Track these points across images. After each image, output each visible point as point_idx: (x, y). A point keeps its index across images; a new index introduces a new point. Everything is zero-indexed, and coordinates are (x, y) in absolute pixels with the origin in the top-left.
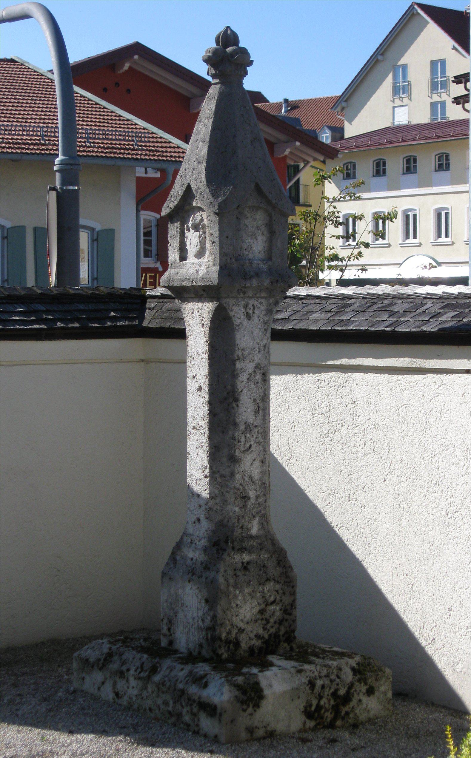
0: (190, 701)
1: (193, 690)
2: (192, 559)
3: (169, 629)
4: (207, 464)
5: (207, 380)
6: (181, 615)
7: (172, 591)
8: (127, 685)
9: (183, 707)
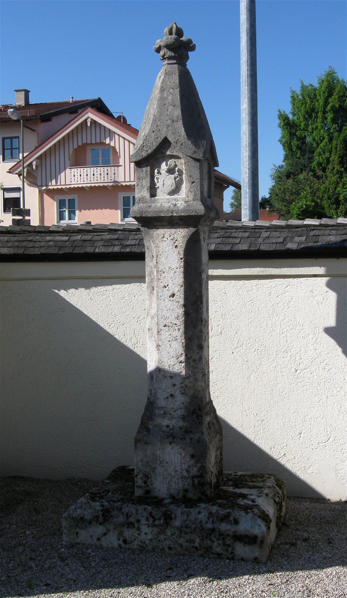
0: (223, 536)
1: (224, 527)
2: (168, 426)
3: (145, 482)
4: (183, 353)
5: (183, 288)
6: (160, 470)
7: (149, 452)
8: (138, 532)
9: (213, 542)
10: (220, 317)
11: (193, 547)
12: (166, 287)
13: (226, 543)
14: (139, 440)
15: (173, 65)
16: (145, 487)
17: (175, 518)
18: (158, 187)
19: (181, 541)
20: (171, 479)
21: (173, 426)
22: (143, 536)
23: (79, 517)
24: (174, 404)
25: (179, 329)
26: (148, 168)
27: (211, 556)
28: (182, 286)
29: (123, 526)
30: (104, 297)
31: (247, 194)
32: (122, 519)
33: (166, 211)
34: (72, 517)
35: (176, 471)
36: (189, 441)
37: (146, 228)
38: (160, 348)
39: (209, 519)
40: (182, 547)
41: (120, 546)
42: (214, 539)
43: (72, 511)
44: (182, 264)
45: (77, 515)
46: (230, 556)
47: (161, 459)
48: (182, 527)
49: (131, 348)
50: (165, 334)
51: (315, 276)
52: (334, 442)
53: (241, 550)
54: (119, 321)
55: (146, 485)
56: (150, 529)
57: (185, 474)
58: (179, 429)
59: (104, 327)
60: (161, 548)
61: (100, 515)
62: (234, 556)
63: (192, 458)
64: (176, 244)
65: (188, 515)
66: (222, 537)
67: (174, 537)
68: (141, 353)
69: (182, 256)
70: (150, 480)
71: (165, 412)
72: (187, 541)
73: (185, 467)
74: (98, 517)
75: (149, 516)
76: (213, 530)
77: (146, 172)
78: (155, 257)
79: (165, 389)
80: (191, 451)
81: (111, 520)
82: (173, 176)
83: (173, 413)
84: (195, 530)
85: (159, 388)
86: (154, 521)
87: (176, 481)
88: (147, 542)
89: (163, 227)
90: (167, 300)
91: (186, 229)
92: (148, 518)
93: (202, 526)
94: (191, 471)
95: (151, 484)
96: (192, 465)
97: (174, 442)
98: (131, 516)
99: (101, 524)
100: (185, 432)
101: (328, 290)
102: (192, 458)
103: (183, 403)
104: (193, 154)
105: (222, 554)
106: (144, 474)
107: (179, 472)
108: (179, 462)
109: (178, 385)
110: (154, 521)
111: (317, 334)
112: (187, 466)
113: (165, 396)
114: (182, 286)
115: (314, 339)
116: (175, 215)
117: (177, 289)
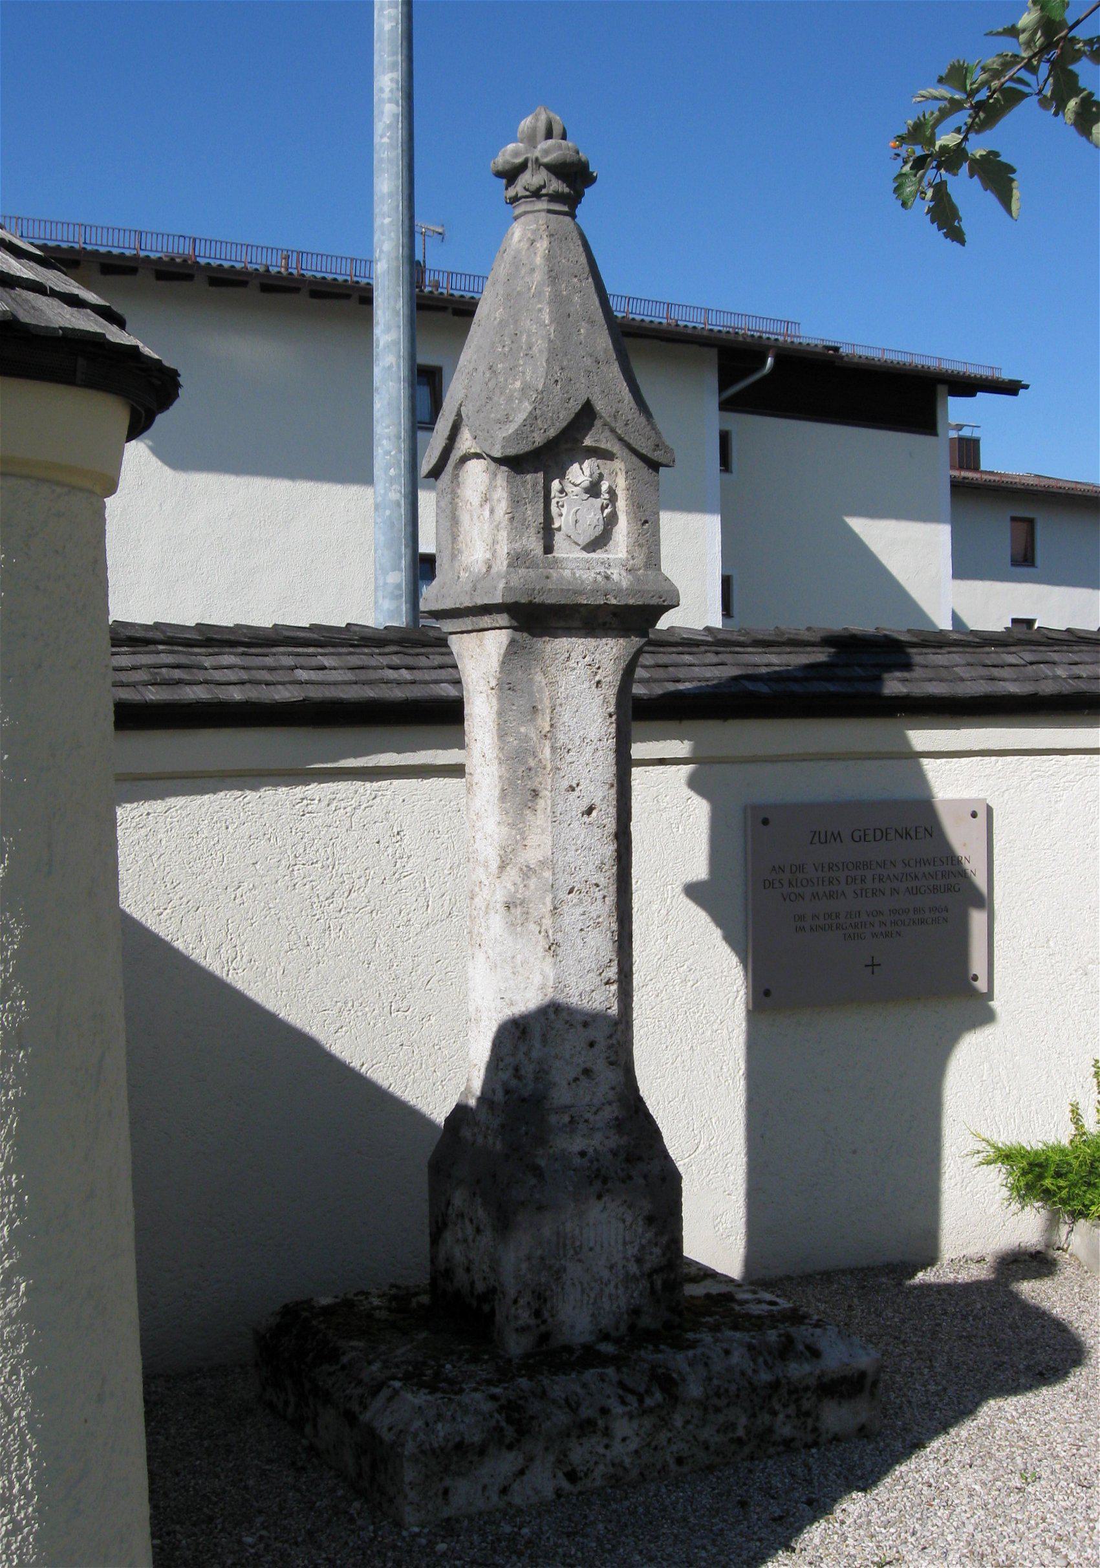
0: (796, 1392)
1: (797, 1370)
2: (583, 1154)
3: (537, 1314)
4: (614, 957)
5: (613, 791)
6: (574, 1270)
7: (547, 1232)
8: (606, 1441)
9: (775, 1413)
10: (446, 872)
11: (732, 1440)
12: (573, 790)
13: (804, 1409)
14: (523, 1203)
15: (561, 217)
16: (538, 1326)
17: (684, 1380)
18: (559, 529)
19: (706, 1434)
20: (602, 1290)
21: (595, 1150)
22: (619, 1450)
23: (450, 1444)
24: (594, 1093)
25: (604, 897)
26: (540, 475)
27: (772, 1450)
28: (612, 786)
29: (568, 1435)
30: (143, 832)
31: (400, 558)
32: (562, 1418)
33: (592, 591)
34: (433, 1451)
35: (611, 1267)
36: (641, 1181)
37: (525, 635)
38: (559, 951)
39: (754, 1360)
40: (707, 1448)
41: (559, 1493)
42: (777, 1407)
43: (421, 1434)
44: (613, 729)
45: (441, 1439)
46: (810, 1439)
47: (578, 1243)
48: (707, 1398)
49: (218, 973)
50: (572, 916)
51: (662, 762)
52: (708, 1152)
53: (836, 1416)
54: (185, 900)
55: (539, 1322)
56: (635, 1424)
57: (633, 1268)
58: (611, 1157)
59: (143, 920)
60: (659, 1467)
61: (503, 1424)
62: (819, 1436)
63: (650, 1225)
64: (597, 678)
65: (706, 1364)
66: (794, 1396)
67: (690, 1427)
68: (246, 984)
69: (612, 709)
70: (549, 1305)
71: (572, 1117)
72: (718, 1431)
73: (632, 1251)
74: (498, 1429)
75: (620, 1392)
76: (775, 1386)
77: (535, 485)
78: (548, 711)
79: (572, 1056)
80: (646, 1206)
81: (537, 1429)
82: (598, 502)
83: (592, 1118)
84: (738, 1396)
85: (556, 1057)
86: (641, 1401)
87: (613, 1291)
88: (627, 1461)
89: (569, 632)
90: (575, 824)
91: (621, 641)
92: (620, 1397)
93: (750, 1383)
94: (647, 1257)
95: (552, 1316)
96: (649, 1242)
97: (608, 1191)
98: (579, 1404)
99: (510, 1447)
100: (628, 1160)
101: (692, 794)
102: (650, 1225)
103: (613, 1088)
104: (655, 450)
105: (793, 1440)
106: (533, 1292)
107: (620, 1267)
108: (620, 1241)
109: (602, 1044)
110: (641, 1401)
111: (669, 901)
112: (636, 1249)
113: (572, 1075)
114: (612, 786)
115: (664, 912)
116: (614, 602)
117: (601, 794)
